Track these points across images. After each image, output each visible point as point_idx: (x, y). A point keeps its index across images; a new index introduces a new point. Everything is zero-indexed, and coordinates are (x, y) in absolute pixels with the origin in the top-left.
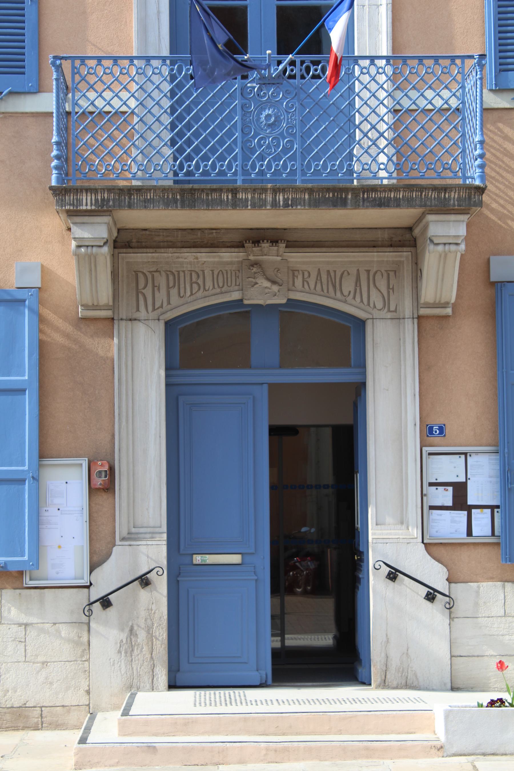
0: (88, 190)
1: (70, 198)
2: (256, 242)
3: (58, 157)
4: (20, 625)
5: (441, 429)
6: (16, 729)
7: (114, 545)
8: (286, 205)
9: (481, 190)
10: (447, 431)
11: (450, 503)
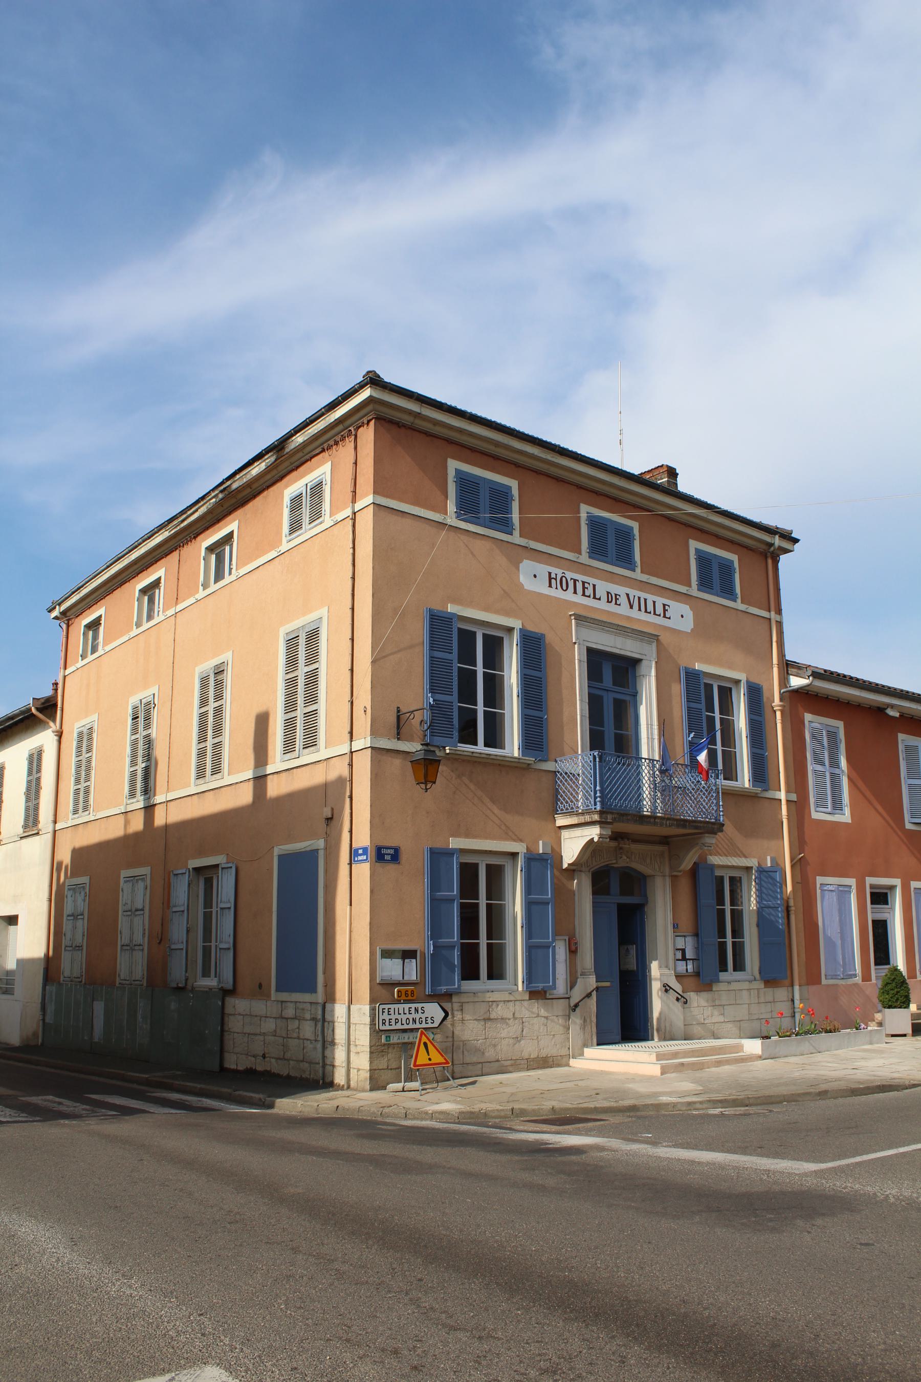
0: (612, 813)
1: (604, 816)
2: (622, 838)
3: (600, 797)
4: (545, 1017)
5: (677, 925)
6: (544, 1068)
7: (577, 978)
8: (669, 826)
9: (723, 825)
10: (679, 926)
11: (681, 958)
